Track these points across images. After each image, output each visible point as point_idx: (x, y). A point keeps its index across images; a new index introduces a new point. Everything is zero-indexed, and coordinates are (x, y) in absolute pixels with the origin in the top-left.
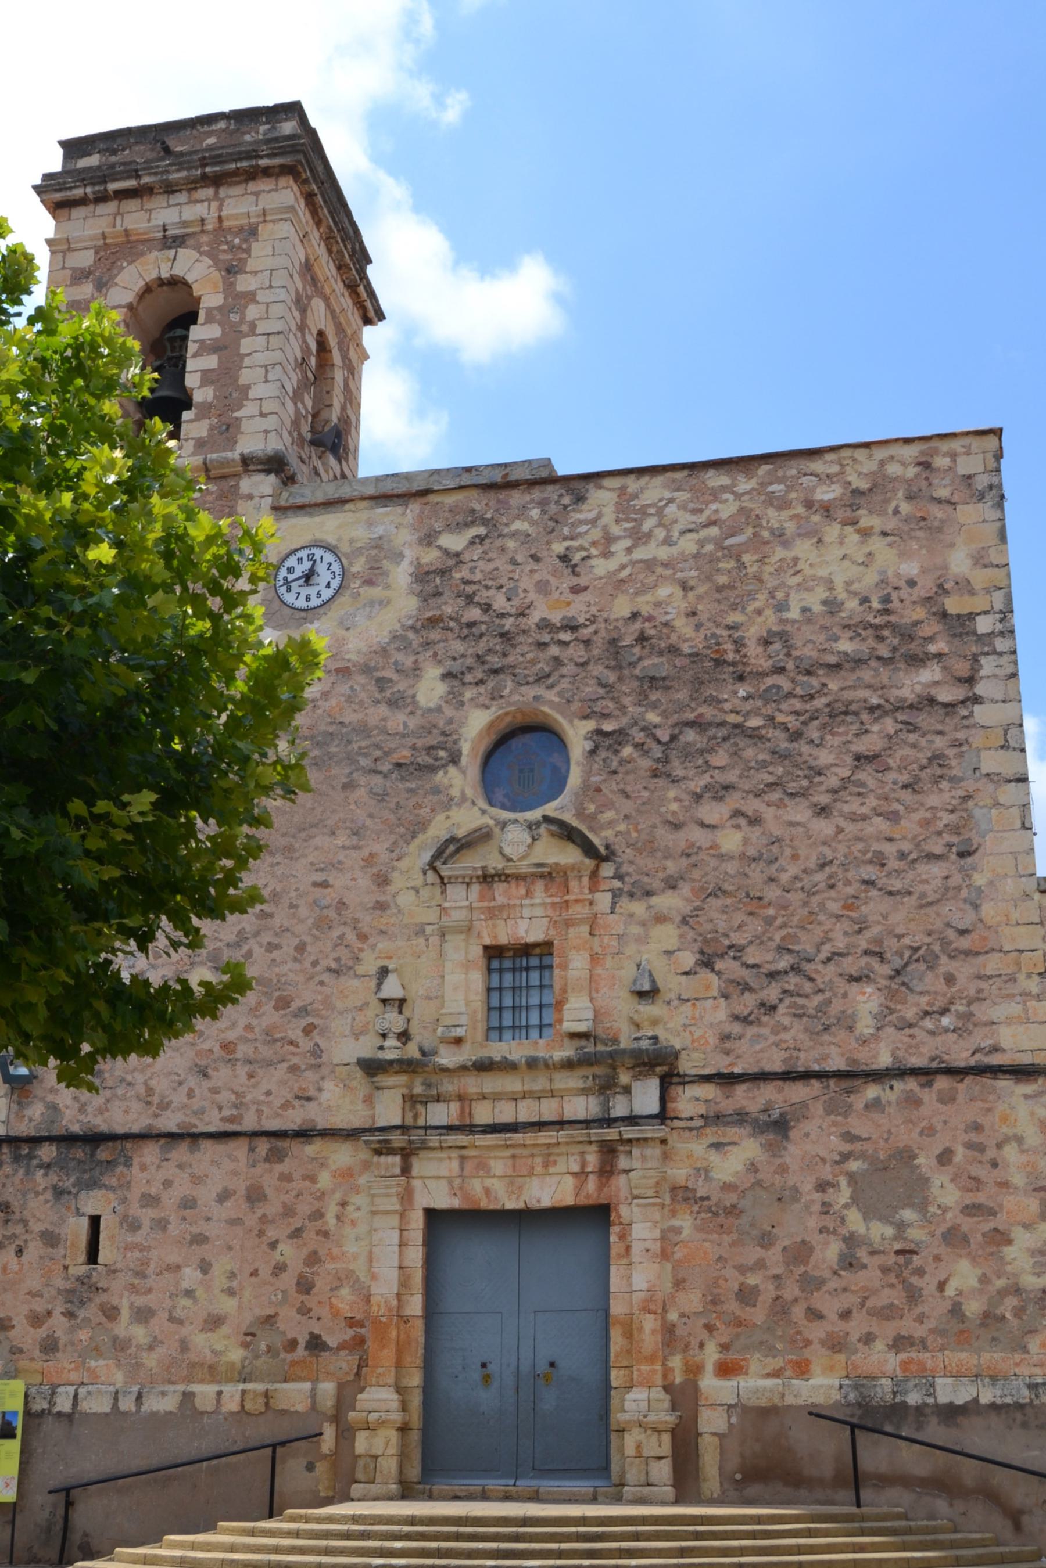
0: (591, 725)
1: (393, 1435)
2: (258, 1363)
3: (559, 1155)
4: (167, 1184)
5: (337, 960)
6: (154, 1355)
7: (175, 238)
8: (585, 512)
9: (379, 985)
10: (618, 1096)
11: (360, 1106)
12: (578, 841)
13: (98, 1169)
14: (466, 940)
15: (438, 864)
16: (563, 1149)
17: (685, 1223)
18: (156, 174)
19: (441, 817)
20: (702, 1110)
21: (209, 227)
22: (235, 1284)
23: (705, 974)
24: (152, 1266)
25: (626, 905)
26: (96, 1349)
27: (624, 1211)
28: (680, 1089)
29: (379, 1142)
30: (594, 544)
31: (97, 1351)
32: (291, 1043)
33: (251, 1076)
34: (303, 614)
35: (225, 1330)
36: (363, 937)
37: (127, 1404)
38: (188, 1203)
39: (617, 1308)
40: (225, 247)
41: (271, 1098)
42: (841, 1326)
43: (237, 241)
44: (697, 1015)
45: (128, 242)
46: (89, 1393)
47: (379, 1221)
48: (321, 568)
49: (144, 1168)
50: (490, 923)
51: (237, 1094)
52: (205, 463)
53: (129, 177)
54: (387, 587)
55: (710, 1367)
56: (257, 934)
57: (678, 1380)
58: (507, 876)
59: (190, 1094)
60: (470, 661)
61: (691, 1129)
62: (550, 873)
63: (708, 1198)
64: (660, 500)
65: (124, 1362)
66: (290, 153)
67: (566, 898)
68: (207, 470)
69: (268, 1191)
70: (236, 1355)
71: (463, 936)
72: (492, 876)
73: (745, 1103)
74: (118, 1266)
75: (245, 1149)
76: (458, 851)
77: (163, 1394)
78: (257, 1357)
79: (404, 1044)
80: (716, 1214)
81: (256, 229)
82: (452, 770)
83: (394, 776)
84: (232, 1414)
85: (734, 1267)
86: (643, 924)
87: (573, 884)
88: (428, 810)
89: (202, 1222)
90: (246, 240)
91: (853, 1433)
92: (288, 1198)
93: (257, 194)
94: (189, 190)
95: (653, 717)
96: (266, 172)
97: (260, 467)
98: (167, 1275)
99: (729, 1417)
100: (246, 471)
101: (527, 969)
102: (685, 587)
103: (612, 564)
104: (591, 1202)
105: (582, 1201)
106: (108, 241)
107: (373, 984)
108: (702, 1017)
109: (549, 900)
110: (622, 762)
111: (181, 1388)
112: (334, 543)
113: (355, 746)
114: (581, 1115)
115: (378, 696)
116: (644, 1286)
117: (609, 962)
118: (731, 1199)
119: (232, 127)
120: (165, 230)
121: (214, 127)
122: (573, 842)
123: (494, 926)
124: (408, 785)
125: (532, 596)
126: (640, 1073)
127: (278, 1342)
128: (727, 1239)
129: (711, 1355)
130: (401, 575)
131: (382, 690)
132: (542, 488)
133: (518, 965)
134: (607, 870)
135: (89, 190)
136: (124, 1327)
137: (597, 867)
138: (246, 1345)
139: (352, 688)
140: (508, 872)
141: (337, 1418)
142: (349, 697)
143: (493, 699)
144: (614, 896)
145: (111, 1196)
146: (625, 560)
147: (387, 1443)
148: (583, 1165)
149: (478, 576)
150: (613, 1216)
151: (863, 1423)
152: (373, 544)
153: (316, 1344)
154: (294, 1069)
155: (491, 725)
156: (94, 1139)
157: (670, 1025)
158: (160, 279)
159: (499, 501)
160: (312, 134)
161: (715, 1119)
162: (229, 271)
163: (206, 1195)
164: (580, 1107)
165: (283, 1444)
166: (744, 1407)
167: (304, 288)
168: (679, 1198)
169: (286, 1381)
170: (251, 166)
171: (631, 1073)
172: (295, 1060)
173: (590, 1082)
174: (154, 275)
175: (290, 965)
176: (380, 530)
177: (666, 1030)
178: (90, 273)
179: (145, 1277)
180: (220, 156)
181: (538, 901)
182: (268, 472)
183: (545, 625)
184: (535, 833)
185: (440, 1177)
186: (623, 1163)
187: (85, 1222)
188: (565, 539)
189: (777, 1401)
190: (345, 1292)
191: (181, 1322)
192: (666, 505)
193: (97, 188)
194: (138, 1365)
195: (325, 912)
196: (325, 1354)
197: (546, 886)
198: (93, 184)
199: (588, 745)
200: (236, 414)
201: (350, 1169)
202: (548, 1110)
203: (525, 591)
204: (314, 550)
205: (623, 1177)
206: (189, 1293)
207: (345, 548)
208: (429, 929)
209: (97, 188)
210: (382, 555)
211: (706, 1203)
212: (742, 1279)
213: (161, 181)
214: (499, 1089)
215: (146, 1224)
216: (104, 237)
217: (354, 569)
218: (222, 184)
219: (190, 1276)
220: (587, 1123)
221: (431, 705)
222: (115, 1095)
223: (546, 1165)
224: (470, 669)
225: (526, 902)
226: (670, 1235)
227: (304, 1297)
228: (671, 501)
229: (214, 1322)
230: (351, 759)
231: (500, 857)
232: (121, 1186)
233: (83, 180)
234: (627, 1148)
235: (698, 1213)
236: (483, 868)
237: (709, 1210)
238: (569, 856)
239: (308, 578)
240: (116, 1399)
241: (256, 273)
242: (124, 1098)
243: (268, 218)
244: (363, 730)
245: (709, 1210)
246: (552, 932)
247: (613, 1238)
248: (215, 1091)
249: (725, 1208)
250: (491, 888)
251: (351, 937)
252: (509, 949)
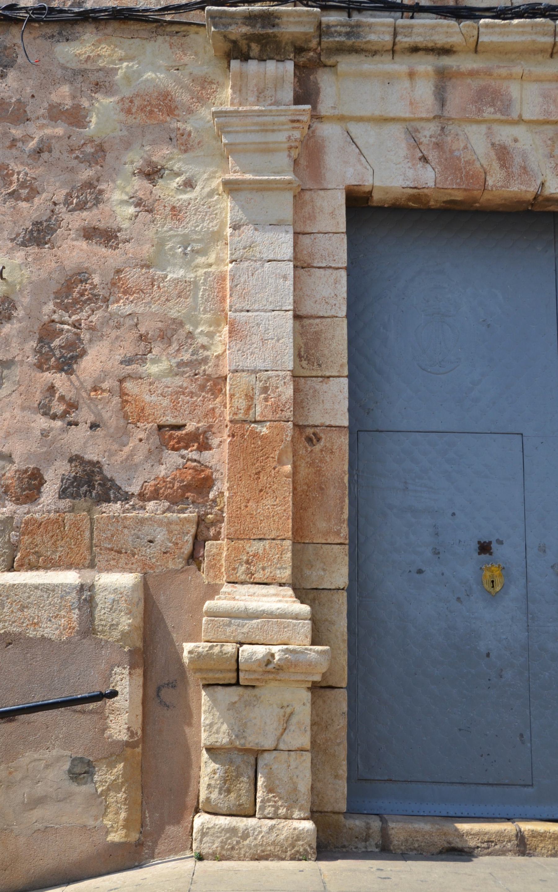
29: (250, 18)
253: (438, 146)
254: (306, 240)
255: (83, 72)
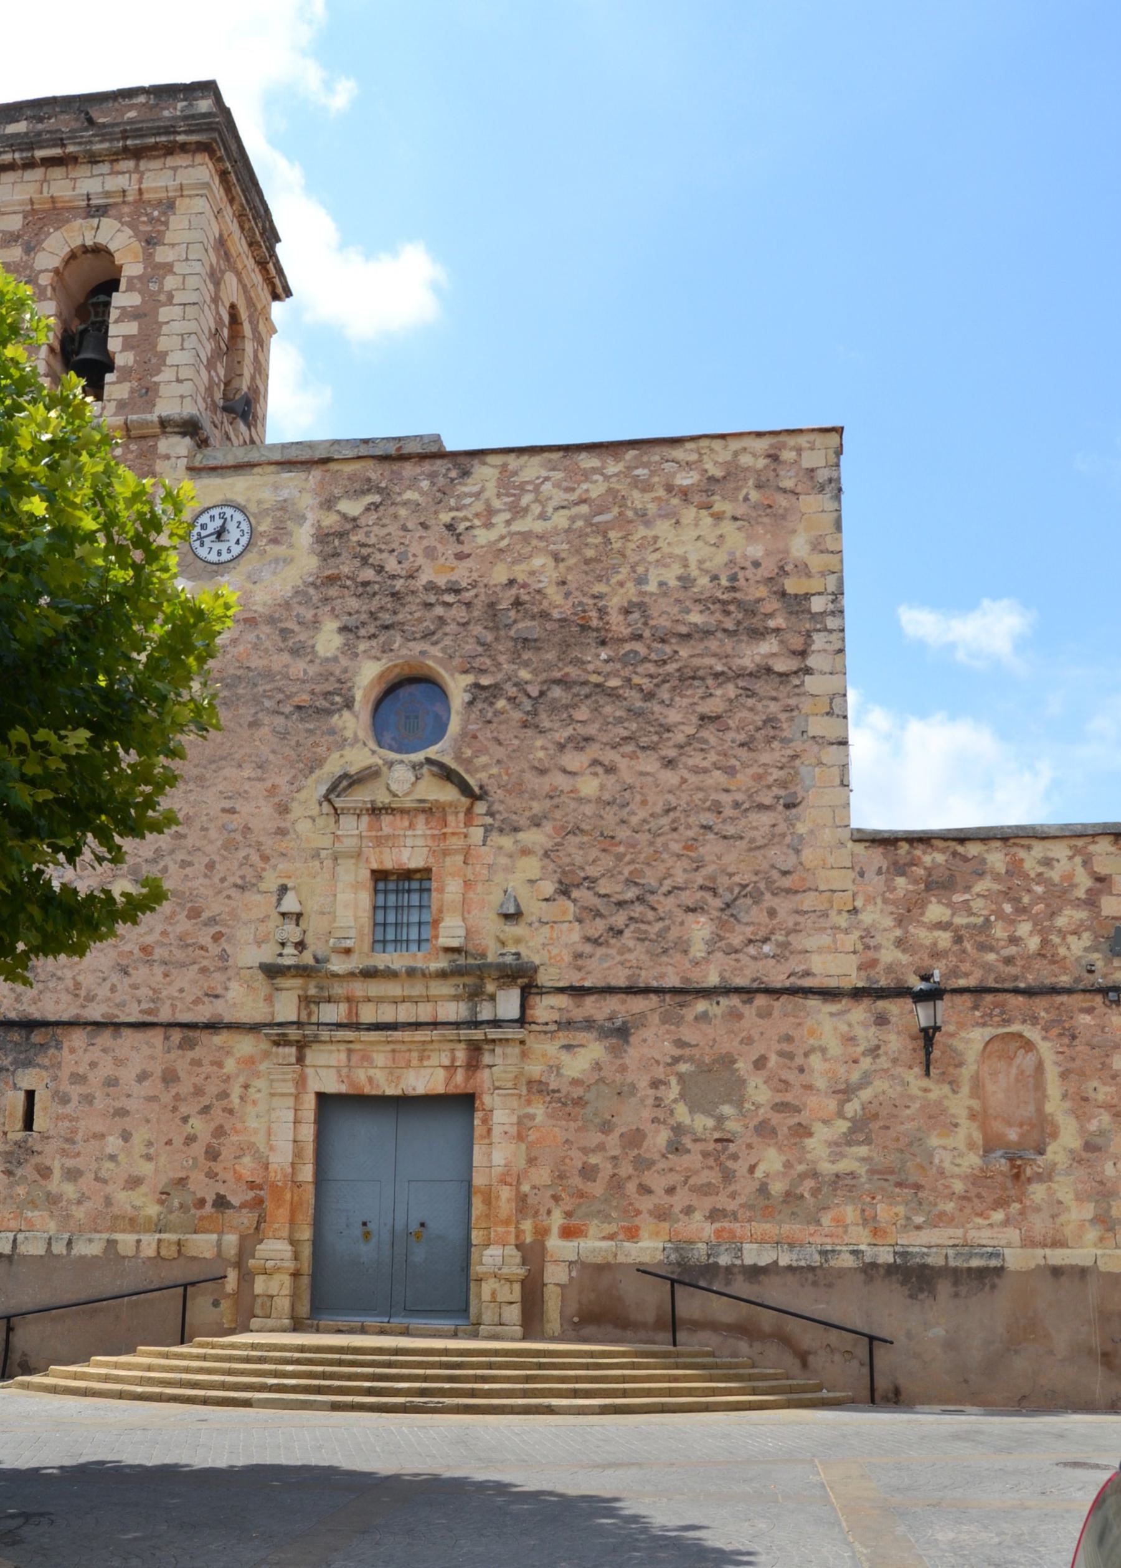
0: (470, 679)
1: (287, 1280)
2: (172, 1217)
3: (432, 1050)
4: (93, 1065)
5: (243, 877)
6: (82, 1209)
7: (98, 208)
8: (469, 486)
9: (279, 900)
10: (485, 1003)
11: (262, 1004)
12: (456, 781)
13: (33, 1050)
14: (356, 864)
15: (332, 797)
16: (436, 1046)
17: (538, 1110)
18: (80, 144)
19: (336, 755)
20: (556, 1016)
21: (130, 198)
22: (152, 1151)
23: (562, 901)
24: (80, 1134)
25: (496, 839)
26: (32, 1202)
27: (487, 1099)
28: (538, 998)
30: (477, 515)
31: (33, 1204)
32: (202, 948)
33: (166, 975)
34: (215, 567)
35: (143, 1189)
36: (265, 858)
37: (59, 1248)
38: (111, 1082)
39: (478, 1180)
40: (145, 219)
41: (184, 994)
42: (667, 1200)
43: (156, 213)
44: (555, 936)
45: (55, 209)
46: (26, 1238)
47: (276, 1102)
48: (231, 526)
49: (72, 1051)
50: (377, 850)
51: (154, 991)
52: (126, 423)
53: (54, 146)
54: (291, 546)
55: (555, 1231)
56: (172, 852)
57: (528, 1240)
58: (393, 809)
59: (113, 989)
60: (364, 617)
61: (546, 1033)
62: (431, 809)
63: (558, 1091)
64: (538, 478)
65: (56, 1213)
66: (206, 130)
67: (444, 830)
68: (128, 430)
69: (181, 1074)
70: (153, 1210)
71: (353, 861)
72: (380, 809)
73: (593, 1012)
74: (51, 1133)
75: (161, 1037)
76: (350, 785)
77: (90, 1240)
78: (171, 1212)
79: (301, 952)
80: (565, 1104)
81: (174, 203)
82: (346, 714)
83: (294, 717)
84: (149, 1258)
85: (579, 1149)
86: (511, 856)
87: (451, 819)
88: (324, 748)
89: (124, 1098)
90: (164, 214)
91: (672, 1286)
92: (199, 1080)
93: (175, 169)
94: (112, 162)
95: (524, 674)
96: (184, 148)
97: (176, 430)
98: (93, 1142)
99: (570, 1271)
100: (164, 433)
101: (409, 891)
102: (557, 558)
103: (493, 535)
104: (459, 1091)
105: (451, 1090)
106: (35, 207)
107: (274, 899)
108: (558, 938)
109: (429, 832)
110: (496, 713)
111: (105, 1236)
112: (243, 503)
113: (261, 689)
114: (452, 1018)
115: (282, 645)
116: (502, 1162)
117: (480, 888)
118: (578, 1092)
119: (152, 102)
120: (89, 199)
121: (135, 101)
122: (452, 782)
123: (381, 853)
124: (307, 726)
125: (421, 560)
126: (504, 984)
127: (189, 1200)
128: (573, 1125)
129: (557, 1220)
130: (304, 535)
131: (284, 640)
132: (432, 461)
133: (401, 888)
134: (481, 808)
135: (17, 155)
136: (55, 1184)
137: (472, 804)
138: (161, 1202)
139: (258, 637)
140: (393, 806)
141: (239, 1264)
142: (256, 644)
143: (384, 652)
144: (486, 831)
145: (44, 1073)
146: (504, 531)
147: (282, 1285)
148: (453, 1059)
149: (372, 540)
150: (477, 1103)
151: (681, 1278)
152: (279, 506)
153: (221, 1202)
154: (204, 970)
155: (381, 676)
156: (29, 1025)
157: (530, 944)
158: (84, 246)
159: (393, 472)
160: (226, 113)
161: (567, 1025)
162: (148, 242)
163: (128, 1075)
164: (452, 1011)
165: (193, 1284)
166: (583, 1263)
167: (218, 262)
168: (534, 1090)
169: (195, 1232)
170: (170, 142)
171: (496, 983)
172: (205, 963)
173: (460, 990)
174: (79, 242)
175: (201, 880)
176: (285, 494)
177: (528, 947)
178: (19, 236)
179: (74, 1143)
180: (141, 129)
181: (419, 832)
182: (184, 434)
183: (431, 587)
184: (418, 772)
185: (329, 1067)
186: (487, 1059)
187: (21, 1096)
188: (451, 510)
189: (610, 1259)
190: (247, 1160)
191: (105, 1182)
192: (542, 483)
193: (25, 155)
194: (69, 1216)
195: (233, 835)
196: (230, 1212)
197: (427, 819)
198: (21, 150)
199: (467, 697)
200: (155, 379)
201: (252, 1057)
202: (424, 1013)
203: (414, 555)
204: (225, 509)
205: (487, 1071)
206: (112, 1158)
207: (253, 508)
208: (323, 854)
209: (25, 155)
210: (286, 517)
211: (557, 1095)
212: (585, 1158)
213: (86, 151)
214: (382, 994)
215: (75, 1098)
216: (32, 202)
217: (261, 529)
218: (143, 158)
219: (113, 1143)
220: (457, 1025)
221: (329, 655)
222: (47, 988)
223: (421, 1059)
224: (363, 624)
225: (409, 833)
226: (526, 1121)
227: (212, 1164)
228: (547, 479)
229: (134, 1182)
230: (256, 701)
231: (387, 793)
232: (53, 1066)
233: (12, 145)
234: (491, 1047)
235: (550, 1103)
236: (372, 802)
237: (559, 1100)
238: (448, 794)
239: (220, 534)
240: (50, 1244)
241: (173, 245)
242: (55, 990)
243: (185, 193)
244: (268, 674)
245: (559, 1100)
246: (431, 860)
247: (476, 1122)
248: (135, 987)
249: (573, 1099)
250: (378, 820)
251: (255, 858)
252: (394, 874)
253: (348, 1076)
254: (299, 1113)
255: (223, 1048)
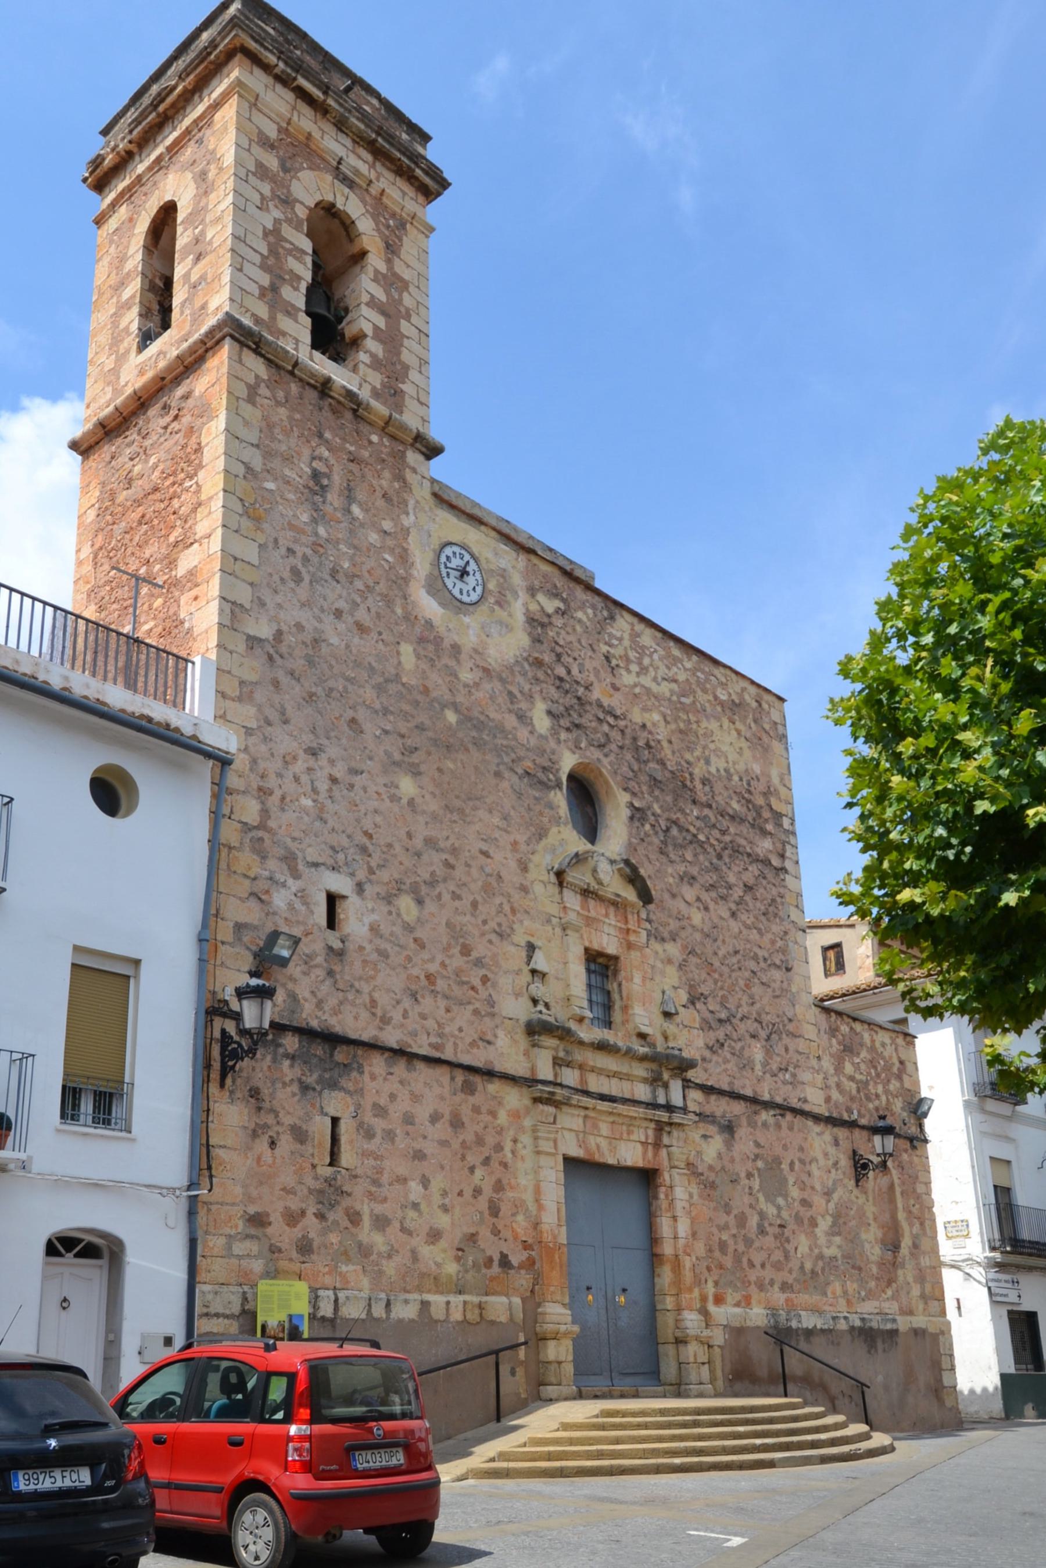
2: (469, 1276)
22: (447, 1201)
24: (386, 1176)
26: (345, 1253)
31: (345, 1255)
35: (443, 1243)
38: (408, 1119)
59: (405, 1015)
65: (369, 1268)
70: (451, 1268)
74: (359, 1171)
78: (467, 1271)
84: (458, 1322)
89: (420, 1139)
98: (397, 1187)
136: (366, 1233)
138: (458, 1259)
163: (422, 1113)
179: (380, 1186)
191: (410, 1233)
194: (381, 1273)
206: (415, 1206)
215: (379, 1133)
219: (415, 1189)
229: (434, 1236)
248: (423, 1017)
